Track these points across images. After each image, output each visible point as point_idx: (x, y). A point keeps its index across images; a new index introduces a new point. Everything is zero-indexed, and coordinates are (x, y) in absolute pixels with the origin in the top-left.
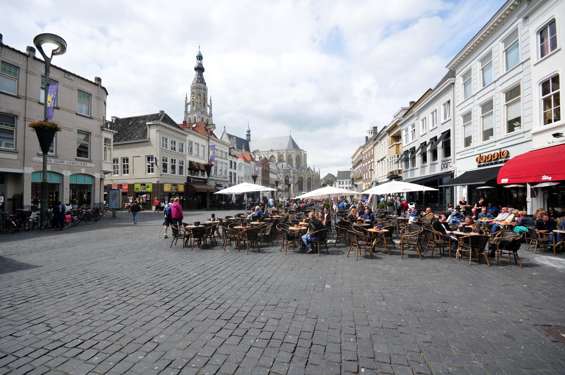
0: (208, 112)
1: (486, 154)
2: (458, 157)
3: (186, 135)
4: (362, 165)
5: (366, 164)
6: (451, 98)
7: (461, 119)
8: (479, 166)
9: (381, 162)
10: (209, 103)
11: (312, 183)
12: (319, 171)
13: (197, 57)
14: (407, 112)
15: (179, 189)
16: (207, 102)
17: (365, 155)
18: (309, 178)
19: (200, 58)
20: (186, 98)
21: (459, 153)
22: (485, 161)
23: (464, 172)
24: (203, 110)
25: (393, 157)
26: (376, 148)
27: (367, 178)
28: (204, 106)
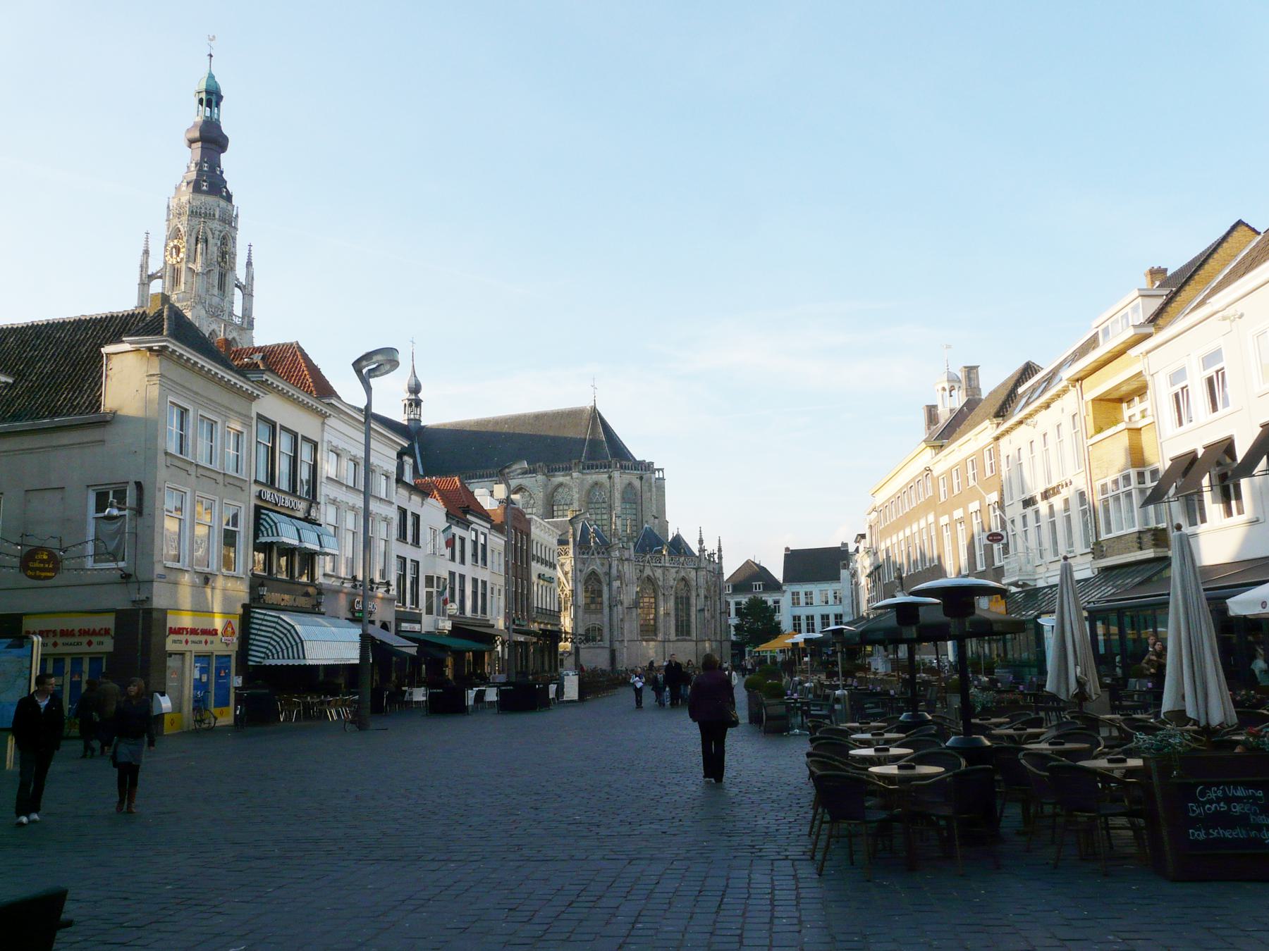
0: (238, 310)
3: (252, 398)
4: (931, 518)
10: (240, 273)
11: (693, 600)
12: (720, 550)
16: (232, 269)
18: (683, 579)
19: (212, 97)
20: (146, 252)
24: (216, 300)
28: (222, 286)
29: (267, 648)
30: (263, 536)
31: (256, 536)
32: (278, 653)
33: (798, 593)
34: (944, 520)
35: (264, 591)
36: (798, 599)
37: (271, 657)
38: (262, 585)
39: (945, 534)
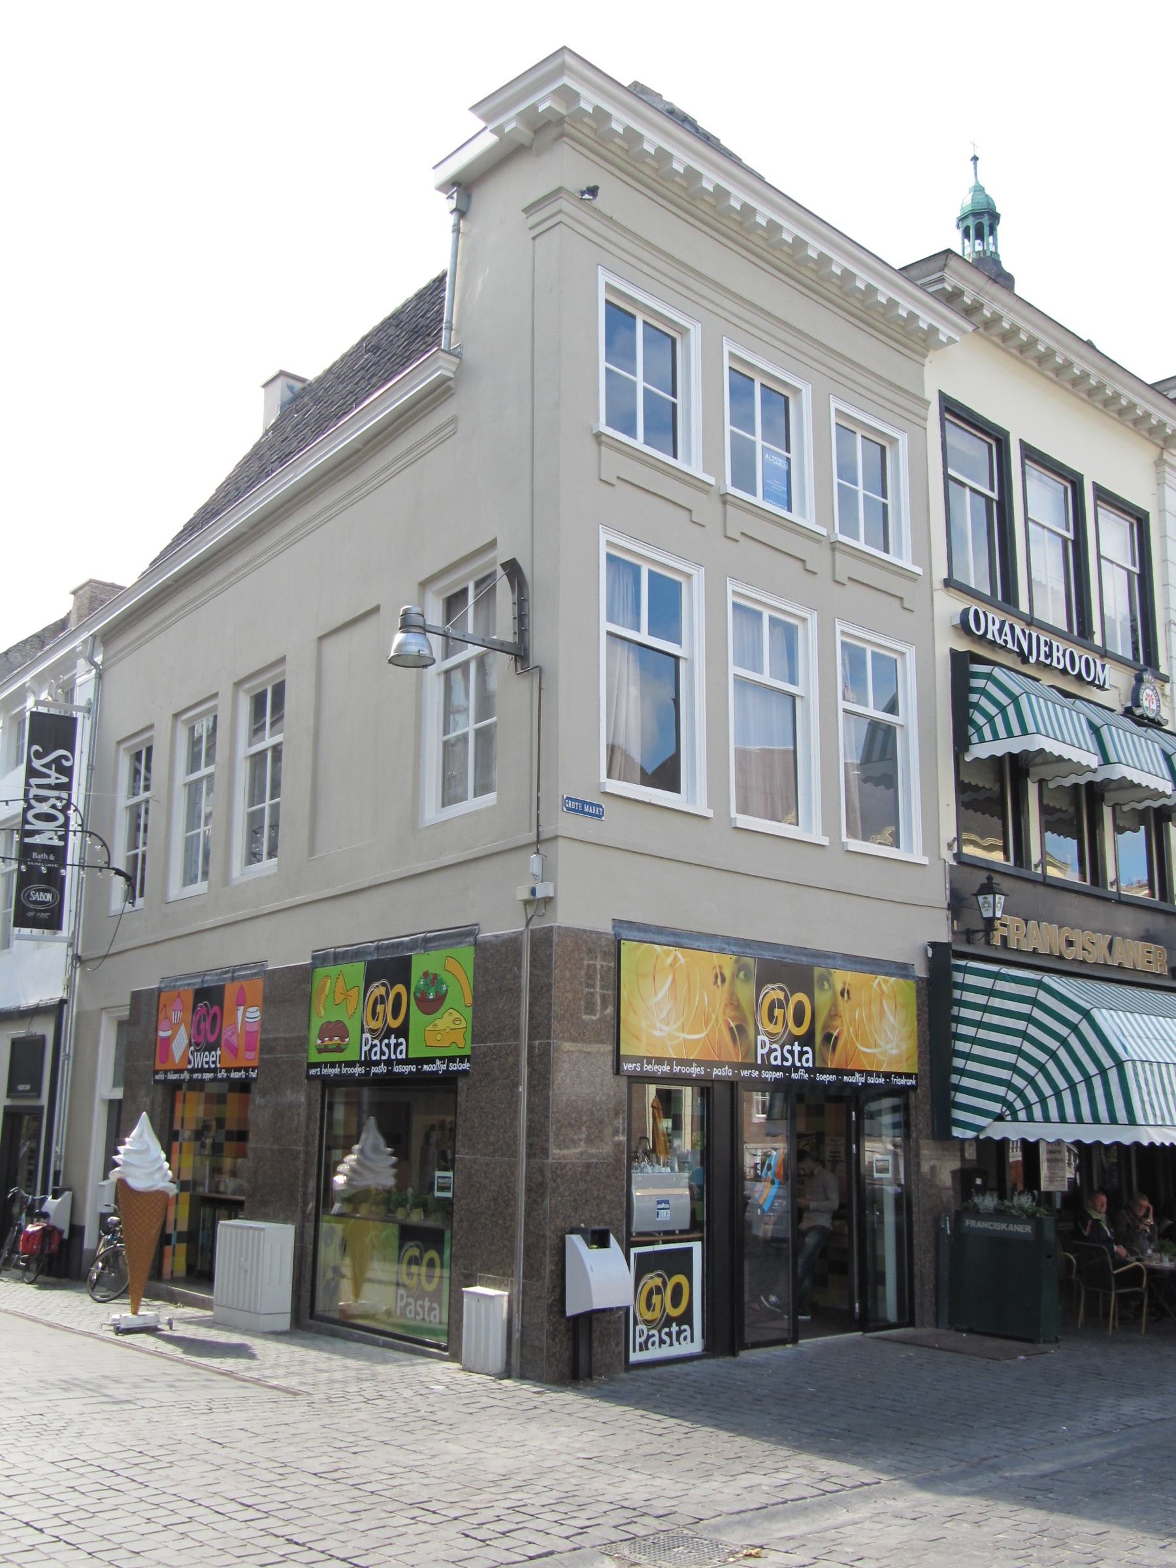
3: (927, 341)
13: (962, 219)
15: (844, 1030)
29: (1008, 1084)
30: (982, 740)
31: (961, 743)
32: (1043, 1100)
35: (995, 906)
37: (1022, 1115)
38: (988, 888)
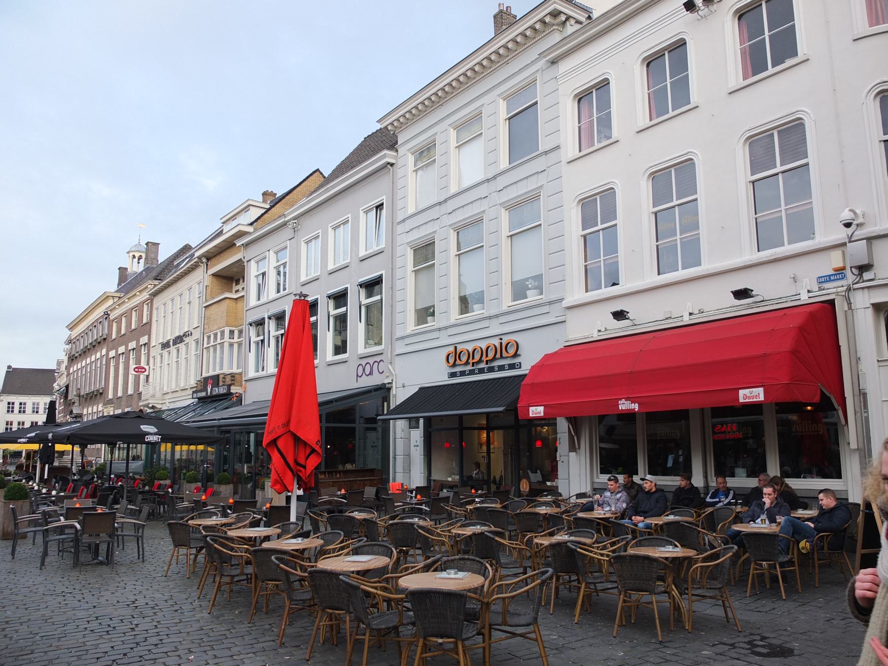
1: (470, 347)
2: (400, 348)
4: (104, 352)
5: (122, 349)
6: (384, 197)
7: (410, 255)
8: (453, 375)
9: (173, 349)
14: (262, 215)
17: (119, 320)
21: (403, 338)
22: (467, 363)
23: (415, 390)
25: (215, 335)
26: (158, 301)
27: (120, 394)
33: (13, 404)
34: (112, 354)
36: (13, 408)
39: (112, 364)
